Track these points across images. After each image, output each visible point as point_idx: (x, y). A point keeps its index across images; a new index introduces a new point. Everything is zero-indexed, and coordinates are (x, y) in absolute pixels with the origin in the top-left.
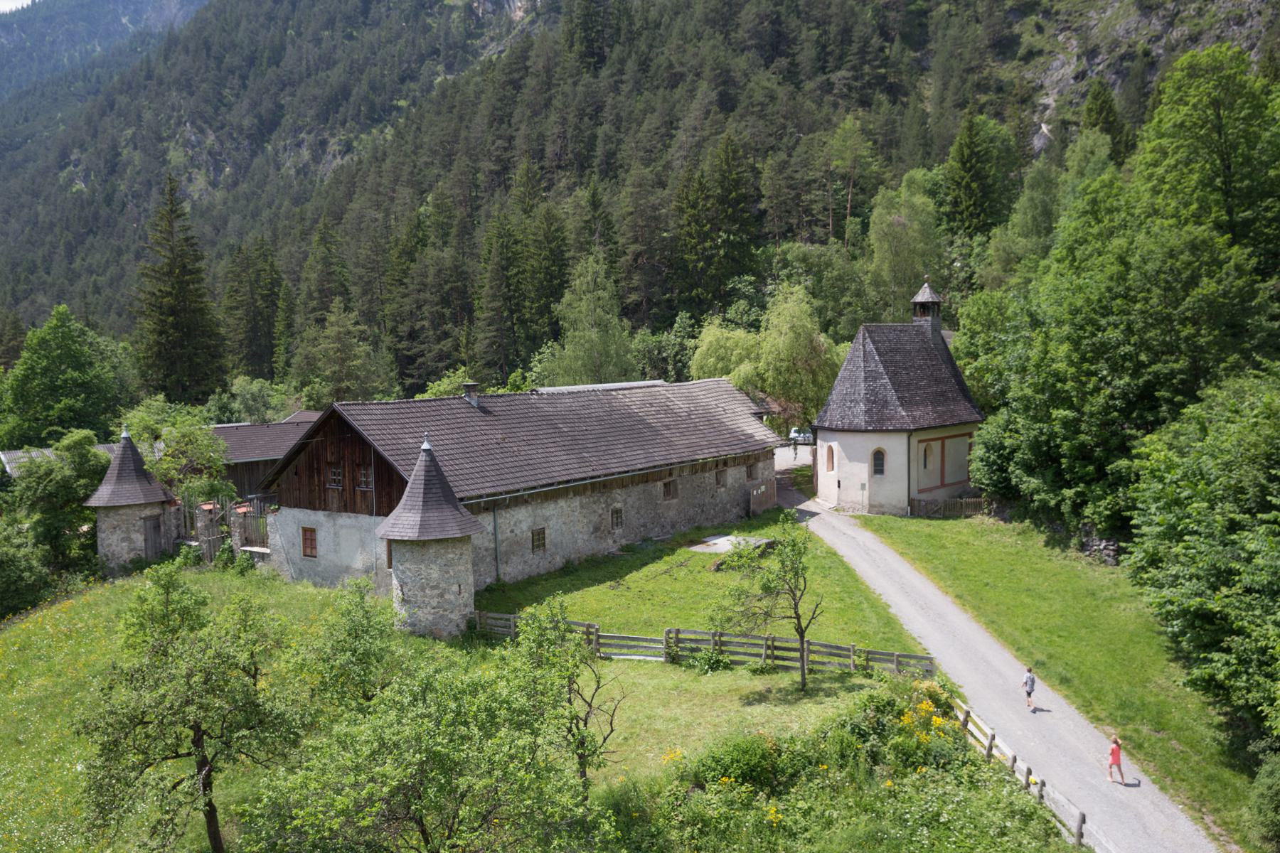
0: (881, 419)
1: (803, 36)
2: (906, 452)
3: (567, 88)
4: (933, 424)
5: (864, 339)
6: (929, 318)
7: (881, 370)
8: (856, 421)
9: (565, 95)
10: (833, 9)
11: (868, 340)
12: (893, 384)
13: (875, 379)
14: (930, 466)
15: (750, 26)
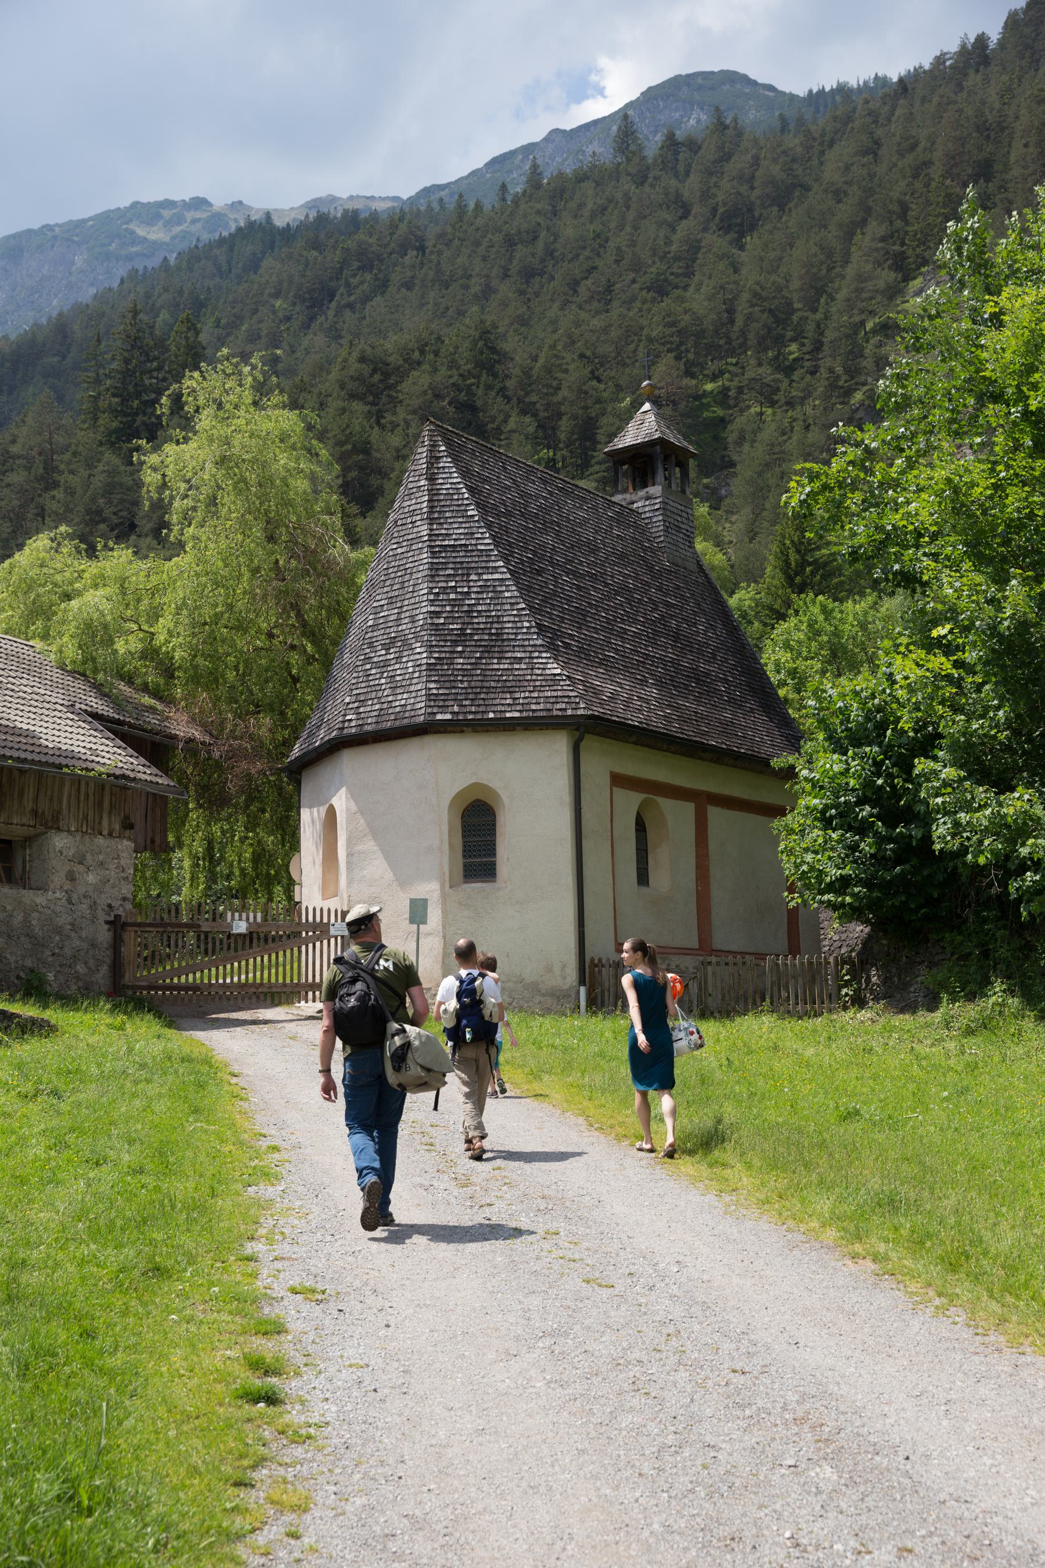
0: (480, 691)
1: (512, 424)
2: (567, 798)
3: (74, 480)
4: (657, 724)
5: (433, 459)
6: (656, 490)
7: (486, 542)
8: (402, 699)
9: (70, 492)
10: (564, 393)
11: (446, 462)
12: (526, 590)
13: (464, 572)
14: (661, 877)
15: (416, 402)
